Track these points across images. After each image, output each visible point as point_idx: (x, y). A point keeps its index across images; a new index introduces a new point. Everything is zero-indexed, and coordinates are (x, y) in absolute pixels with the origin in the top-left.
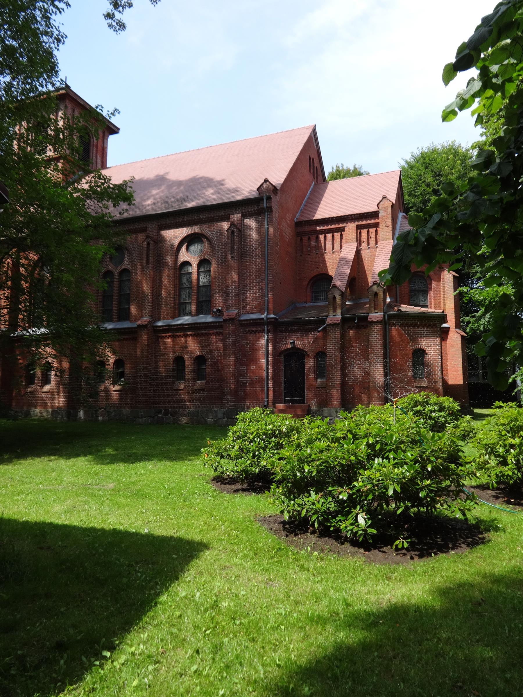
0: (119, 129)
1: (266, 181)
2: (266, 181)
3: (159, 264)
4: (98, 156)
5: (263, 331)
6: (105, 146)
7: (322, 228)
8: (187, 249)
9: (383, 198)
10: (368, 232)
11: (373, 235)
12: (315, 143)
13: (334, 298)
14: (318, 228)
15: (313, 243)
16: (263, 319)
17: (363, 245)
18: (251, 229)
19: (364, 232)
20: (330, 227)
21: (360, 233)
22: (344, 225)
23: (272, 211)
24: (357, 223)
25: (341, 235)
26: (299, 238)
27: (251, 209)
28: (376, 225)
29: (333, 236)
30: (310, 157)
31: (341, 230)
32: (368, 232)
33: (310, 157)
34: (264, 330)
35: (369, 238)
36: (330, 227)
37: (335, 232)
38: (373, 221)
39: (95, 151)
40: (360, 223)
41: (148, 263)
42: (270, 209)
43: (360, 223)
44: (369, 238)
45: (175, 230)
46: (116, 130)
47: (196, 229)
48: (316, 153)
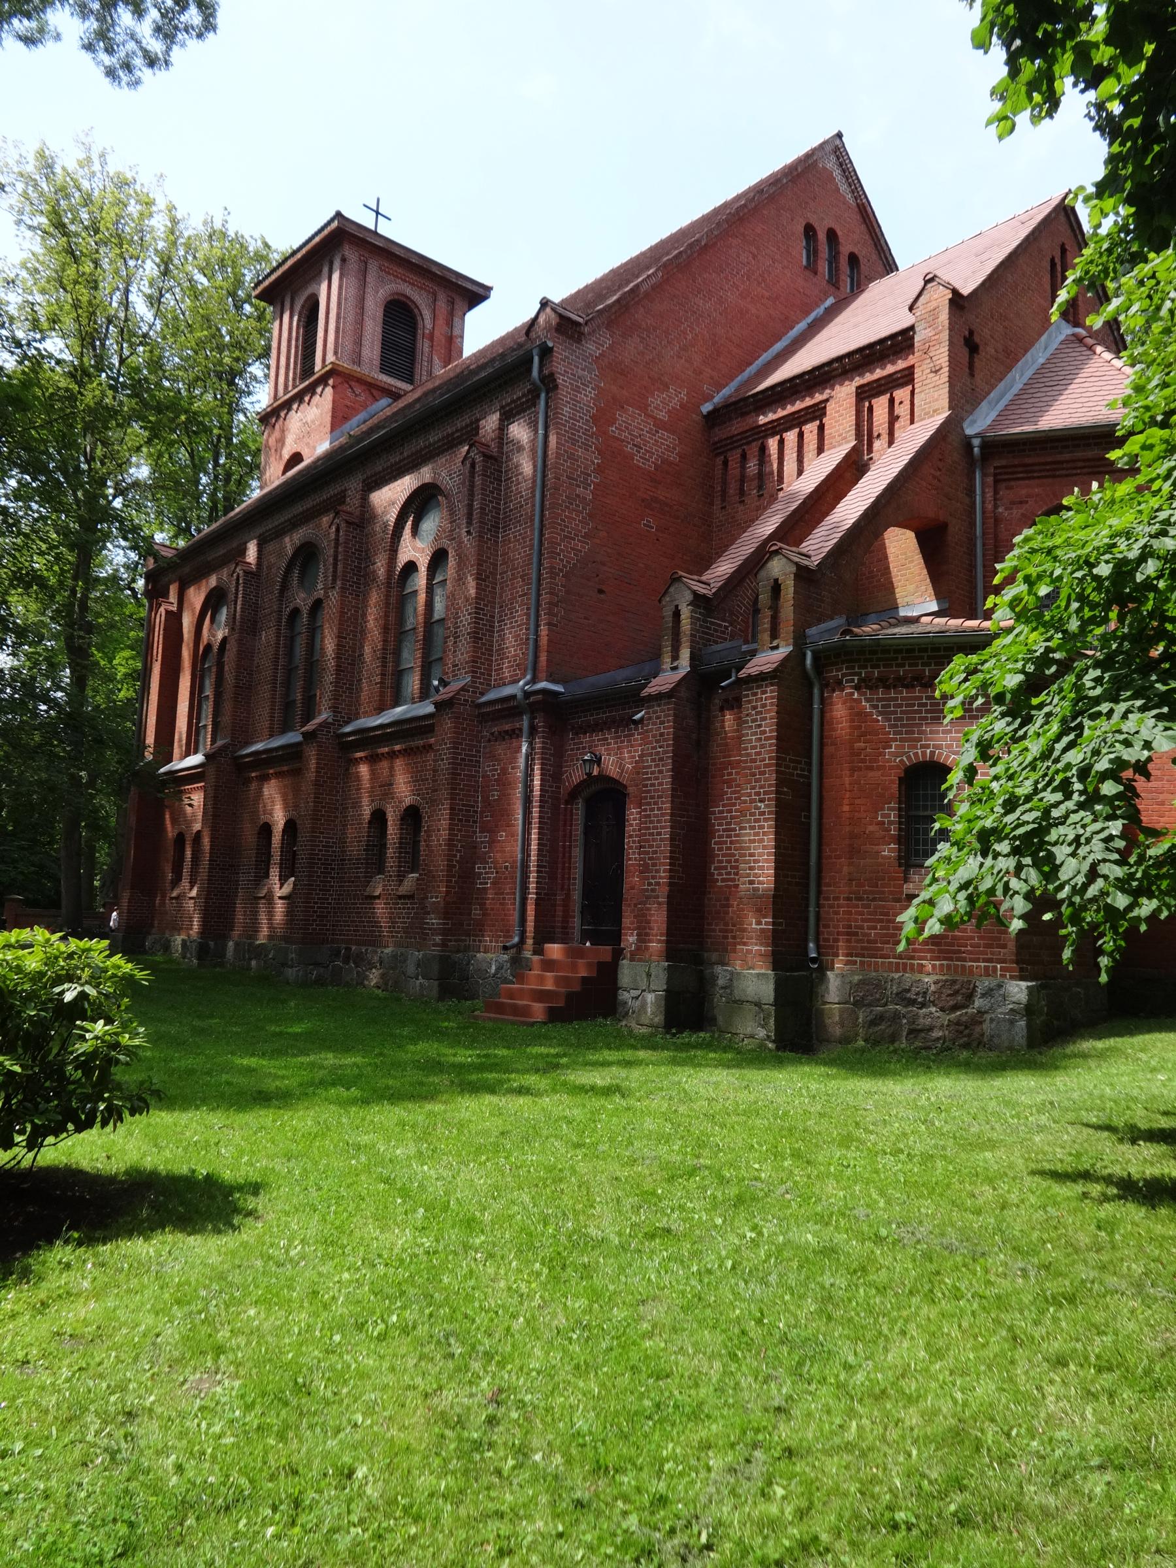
0: (489, 289)
1: (545, 303)
2: (545, 303)
3: (357, 577)
4: (435, 358)
5: (515, 734)
6: (456, 332)
7: (771, 416)
8: (415, 532)
9: (927, 282)
10: (892, 401)
11: (902, 411)
12: (843, 188)
13: (677, 614)
14: (762, 420)
15: (752, 466)
16: (513, 697)
17: (877, 445)
18: (520, 449)
19: (880, 405)
20: (790, 409)
21: (871, 409)
22: (818, 397)
23: (556, 387)
24: (858, 381)
25: (821, 428)
26: (719, 460)
27: (519, 392)
28: (907, 377)
29: (801, 435)
30: (810, 231)
31: (817, 412)
32: (892, 401)
33: (810, 231)
34: (521, 730)
35: (893, 419)
36: (790, 409)
37: (806, 422)
38: (901, 364)
39: (426, 350)
40: (869, 377)
41: (334, 581)
42: (549, 383)
43: (869, 377)
44: (893, 419)
45: (392, 486)
46: (481, 291)
47: (426, 474)
48: (854, 218)
